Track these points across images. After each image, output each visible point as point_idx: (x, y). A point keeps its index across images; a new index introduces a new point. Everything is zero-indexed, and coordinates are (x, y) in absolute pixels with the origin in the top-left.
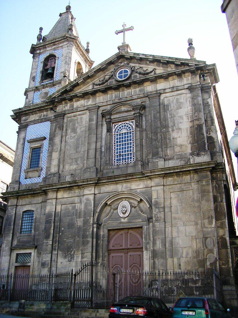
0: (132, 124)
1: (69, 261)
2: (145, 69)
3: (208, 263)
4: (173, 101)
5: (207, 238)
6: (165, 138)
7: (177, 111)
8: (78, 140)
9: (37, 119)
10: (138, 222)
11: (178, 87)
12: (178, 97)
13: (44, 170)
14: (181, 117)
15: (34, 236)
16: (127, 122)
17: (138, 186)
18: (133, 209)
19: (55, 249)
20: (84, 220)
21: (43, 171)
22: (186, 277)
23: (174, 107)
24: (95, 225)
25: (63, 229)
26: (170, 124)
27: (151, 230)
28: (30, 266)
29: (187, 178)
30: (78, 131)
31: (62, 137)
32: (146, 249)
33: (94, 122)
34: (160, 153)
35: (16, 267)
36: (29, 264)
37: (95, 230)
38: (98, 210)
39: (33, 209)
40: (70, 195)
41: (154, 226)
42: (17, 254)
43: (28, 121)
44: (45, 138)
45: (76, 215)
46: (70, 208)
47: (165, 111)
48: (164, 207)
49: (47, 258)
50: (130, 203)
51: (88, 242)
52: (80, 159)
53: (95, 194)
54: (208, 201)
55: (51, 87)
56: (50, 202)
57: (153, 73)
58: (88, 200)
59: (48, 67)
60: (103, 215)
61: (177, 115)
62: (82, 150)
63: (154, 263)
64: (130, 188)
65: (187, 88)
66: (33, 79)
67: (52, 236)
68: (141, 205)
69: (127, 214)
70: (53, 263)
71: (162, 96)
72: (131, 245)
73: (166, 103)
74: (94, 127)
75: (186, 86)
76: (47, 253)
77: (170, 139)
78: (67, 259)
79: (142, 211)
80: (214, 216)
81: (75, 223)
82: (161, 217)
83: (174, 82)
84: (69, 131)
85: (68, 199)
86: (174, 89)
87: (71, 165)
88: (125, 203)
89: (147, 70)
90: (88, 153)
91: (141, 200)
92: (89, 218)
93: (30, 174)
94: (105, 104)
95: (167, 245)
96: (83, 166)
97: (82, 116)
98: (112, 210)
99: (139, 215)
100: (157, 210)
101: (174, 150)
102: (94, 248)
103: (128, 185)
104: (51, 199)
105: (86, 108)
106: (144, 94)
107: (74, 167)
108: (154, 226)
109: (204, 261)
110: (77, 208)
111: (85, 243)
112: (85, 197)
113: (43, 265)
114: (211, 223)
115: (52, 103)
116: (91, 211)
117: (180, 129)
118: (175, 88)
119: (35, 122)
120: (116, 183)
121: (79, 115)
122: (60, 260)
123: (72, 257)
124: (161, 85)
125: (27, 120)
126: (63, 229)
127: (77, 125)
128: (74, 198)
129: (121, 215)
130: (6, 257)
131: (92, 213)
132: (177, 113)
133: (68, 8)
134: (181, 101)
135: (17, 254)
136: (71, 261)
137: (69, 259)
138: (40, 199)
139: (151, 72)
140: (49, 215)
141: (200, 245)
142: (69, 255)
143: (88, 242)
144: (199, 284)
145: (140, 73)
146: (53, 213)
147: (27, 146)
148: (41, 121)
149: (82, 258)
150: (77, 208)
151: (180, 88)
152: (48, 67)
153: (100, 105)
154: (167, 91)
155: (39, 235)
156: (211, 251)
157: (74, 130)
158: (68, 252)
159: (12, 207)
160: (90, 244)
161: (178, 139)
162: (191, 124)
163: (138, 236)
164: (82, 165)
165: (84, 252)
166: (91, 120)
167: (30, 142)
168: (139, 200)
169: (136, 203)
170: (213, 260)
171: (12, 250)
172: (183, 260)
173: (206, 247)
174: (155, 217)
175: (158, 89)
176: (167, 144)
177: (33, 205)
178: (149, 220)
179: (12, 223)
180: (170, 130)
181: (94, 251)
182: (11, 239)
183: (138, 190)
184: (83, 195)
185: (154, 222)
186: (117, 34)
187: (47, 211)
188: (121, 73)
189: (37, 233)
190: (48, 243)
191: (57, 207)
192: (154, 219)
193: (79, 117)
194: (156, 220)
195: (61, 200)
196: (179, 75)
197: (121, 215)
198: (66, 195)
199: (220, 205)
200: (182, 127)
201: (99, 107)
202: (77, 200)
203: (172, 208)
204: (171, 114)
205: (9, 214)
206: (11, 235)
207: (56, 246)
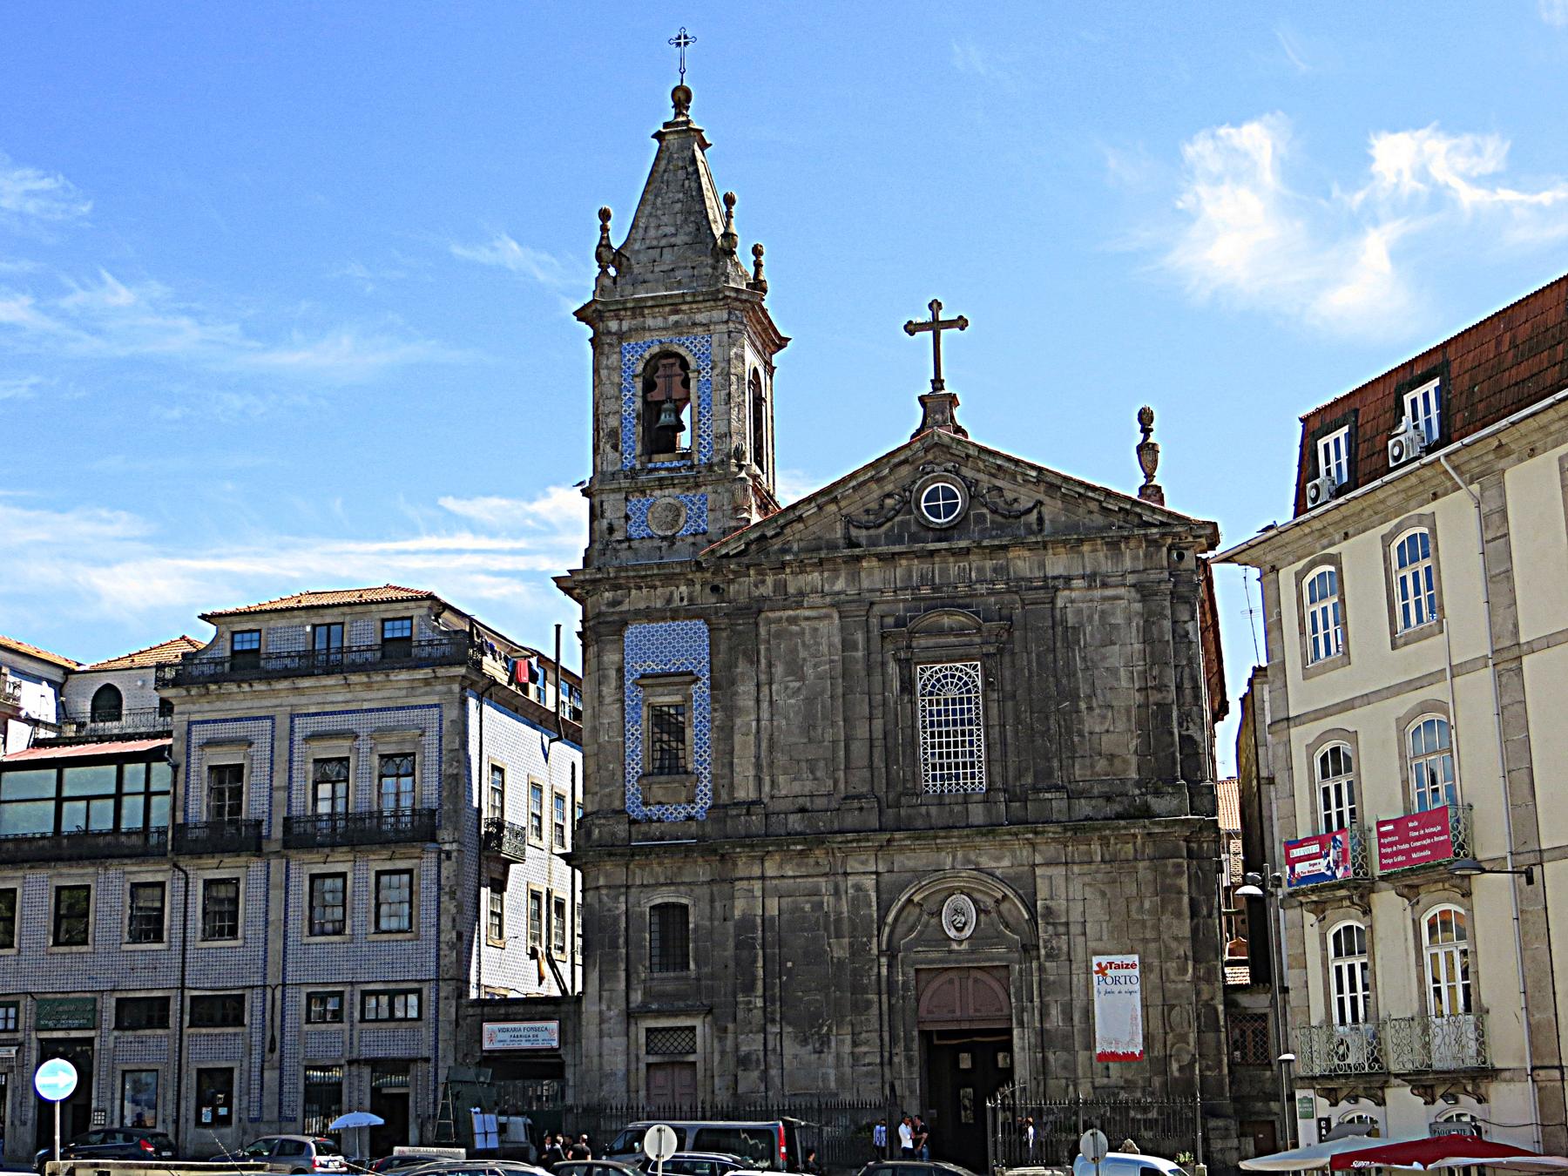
0: (973, 673)
2: (1009, 496)
3: (1175, 1066)
4: (1090, 618)
5: (1172, 1007)
6: (1069, 731)
7: (1103, 650)
8: (810, 701)
12: (1106, 606)
13: (705, 782)
14: (1113, 671)
15: (698, 979)
17: (1000, 859)
18: (982, 916)
19: (773, 1021)
20: (851, 945)
22: (1123, 1095)
23: (1092, 635)
24: (884, 960)
25: (789, 964)
27: (1035, 979)
28: (694, 1063)
30: (809, 671)
31: (758, 685)
32: (1021, 1024)
35: (649, 1066)
36: (691, 1058)
37: (884, 971)
38: (890, 919)
39: (684, 901)
40: (803, 871)
41: (1041, 969)
42: (648, 1030)
44: (691, 677)
45: (826, 929)
46: (808, 907)
47: (1069, 646)
48: (1067, 924)
49: (752, 1044)
50: (975, 902)
51: (869, 1004)
52: (822, 764)
53: (877, 873)
54: (1178, 914)
57: (1034, 515)
59: (656, 395)
60: (900, 930)
61: (1101, 665)
62: (828, 737)
63: (1044, 1059)
64: (977, 864)
65: (1134, 586)
66: (605, 438)
67: (760, 984)
68: (1005, 907)
69: (967, 932)
70: (772, 1058)
71: (1062, 598)
72: (976, 1010)
73: (1071, 620)
74: (860, 667)
75: (1131, 579)
78: (810, 1047)
79: (1007, 926)
80: (1190, 954)
82: (1059, 949)
83: (1095, 557)
84: (779, 670)
89: (1016, 500)
90: (847, 748)
91: (1005, 897)
93: (658, 792)
94: (889, 596)
95: (1076, 1018)
96: (836, 782)
97: (815, 624)
98: (925, 917)
99: (1000, 935)
100: (1050, 928)
101: (1092, 766)
102: (886, 1017)
108: (1041, 969)
109: (1166, 1059)
111: (861, 1007)
112: (851, 880)
113: (744, 1062)
115: (714, 566)
119: (649, 615)
122: (790, 1048)
123: (825, 1041)
124: (1057, 563)
125: (620, 603)
127: (803, 654)
129: (952, 933)
132: (1104, 658)
134: (1119, 619)
135: (648, 1030)
136: (821, 1052)
138: (701, 871)
139: (1030, 511)
140: (746, 924)
143: (869, 1004)
144: (1153, 1114)
146: (759, 921)
147: (633, 694)
149: (855, 1044)
152: (656, 395)
153: (876, 597)
154: (1076, 583)
155: (713, 976)
156: (1183, 1038)
157: (795, 669)
158: (812, 1030)
159: (613, 892)
160: (875, 1010)
162: (1138, 698)
163: (996, 986)
164: (830, 782)
165: (858, 1029)
166: (848, 645)
168: (999, 896)
169: (990, 903)
170: (1186, 1059)
171: (630, 1015)
173: (1172, 1030)
175: (1050, 574)
176: (1073, 749)
178: (1029, 949)
179: (621, 941)
180: (1083, 706)
181: (886, 1028)
182: (623, 985)
183: (998, 873)
184: (846, 874)
187: (737, 913)
188: (932, 496)
189: (706, 970)
190: (750, 1002)
191: (768, 901)
192: (1043, 952)
193: (804, 624)
197: (952, 933)
199: (1205, 924)
200: (1114, 703)
201: (872, 604)
203: (1088, 925)
204: (1084, 659)
206: (623, 975)
207: (773, 1012)
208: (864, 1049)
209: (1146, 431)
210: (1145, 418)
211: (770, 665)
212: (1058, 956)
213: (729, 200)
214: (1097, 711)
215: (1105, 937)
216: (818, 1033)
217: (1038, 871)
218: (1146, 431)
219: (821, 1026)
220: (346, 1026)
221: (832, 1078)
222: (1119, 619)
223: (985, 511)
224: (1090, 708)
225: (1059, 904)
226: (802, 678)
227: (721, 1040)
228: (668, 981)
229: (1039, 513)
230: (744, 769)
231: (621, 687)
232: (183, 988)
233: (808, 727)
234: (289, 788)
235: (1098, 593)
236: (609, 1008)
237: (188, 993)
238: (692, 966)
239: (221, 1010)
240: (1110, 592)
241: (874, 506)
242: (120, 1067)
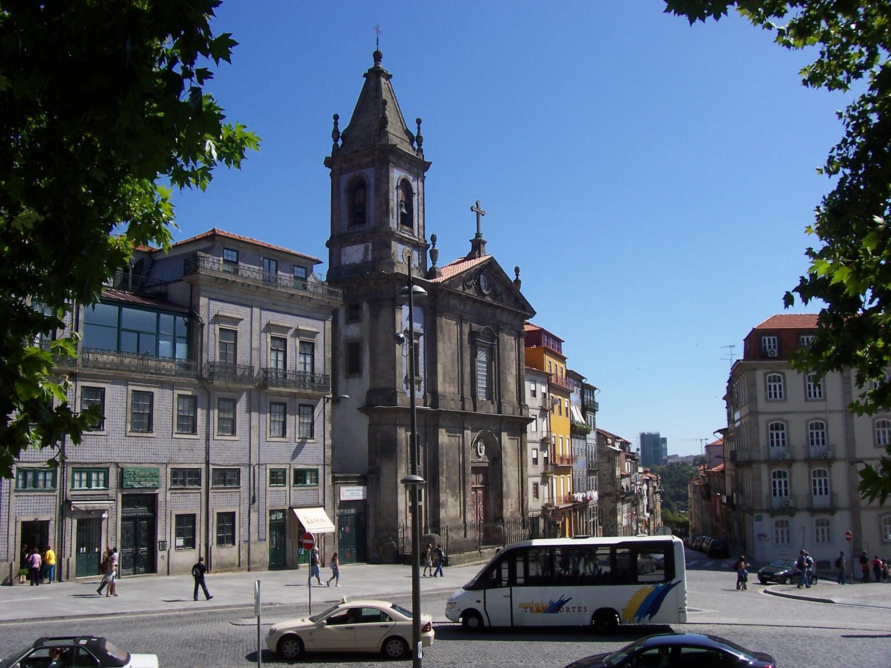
8: (453, 353)
75: (518, 329)
84: (446, 337)
133: (377, 56)
157: (450, 340)
209: (517, 275)
210: (517, 270)
213: (419, 121)
218: (517, 275)
220: (287, 488)
232: (207, 463)
233: (453, 365)
234: (260, 350)
237: (211, 467)
239: (227, 477)
242: (175, 512)
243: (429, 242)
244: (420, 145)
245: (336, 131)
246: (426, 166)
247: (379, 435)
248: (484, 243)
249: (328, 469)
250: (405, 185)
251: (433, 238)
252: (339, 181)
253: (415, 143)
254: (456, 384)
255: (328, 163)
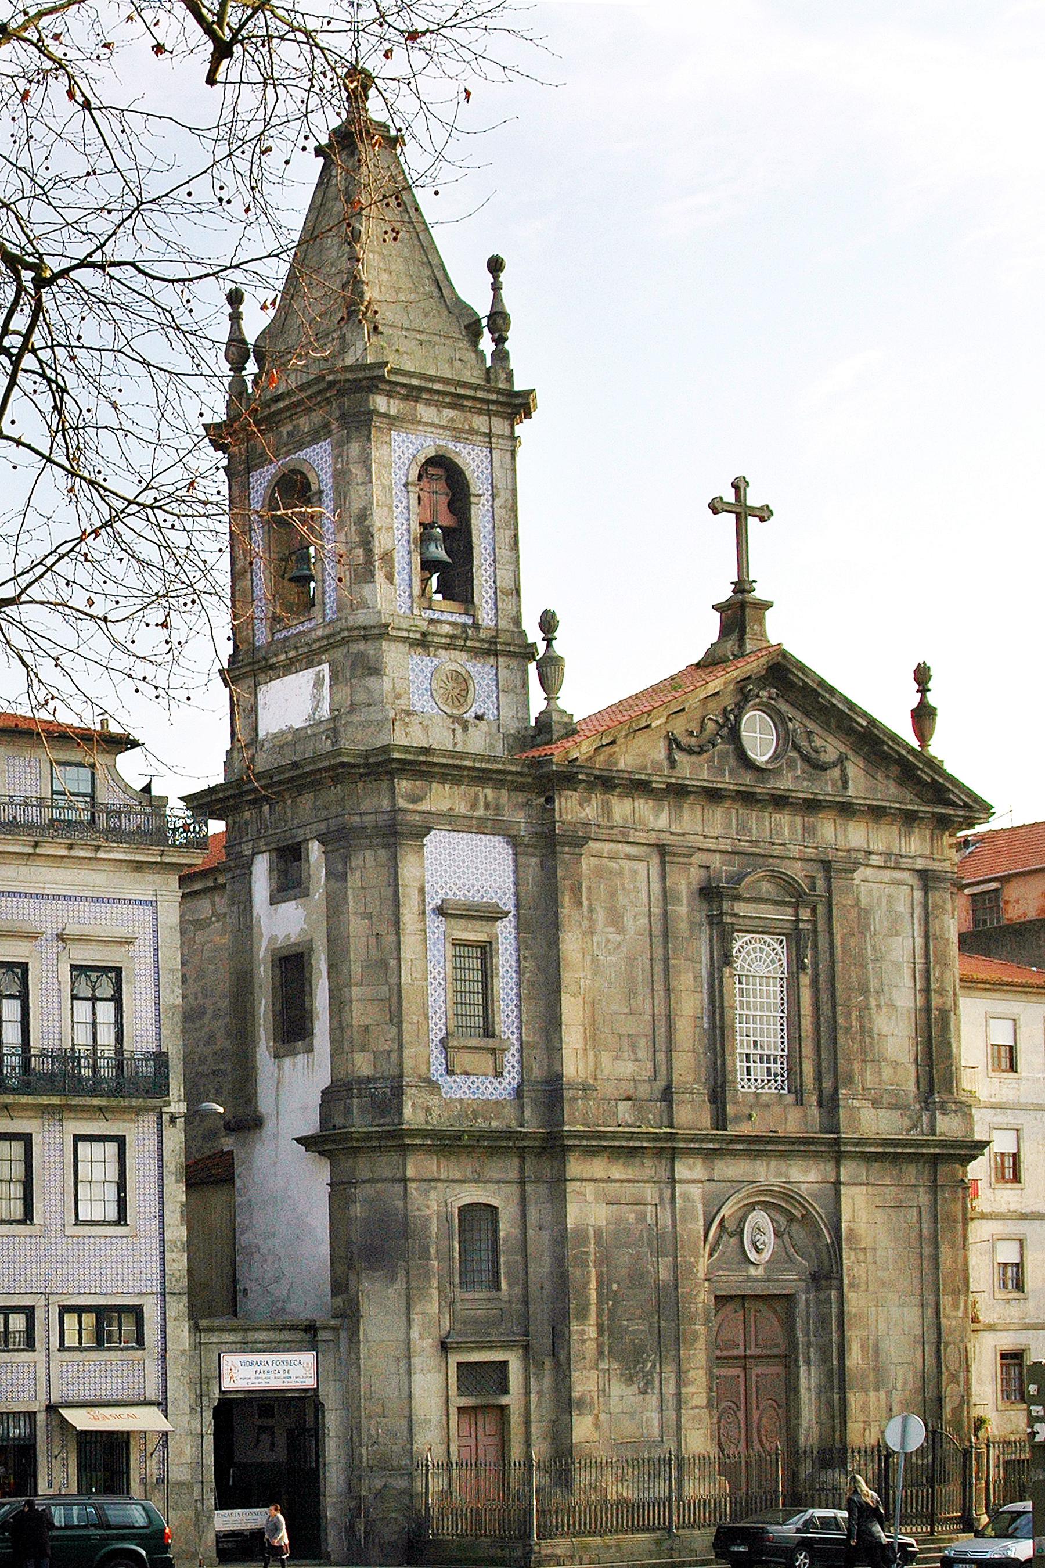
1: (641, 1393)
2: (818, 742)
5: (947, 1344)
8: (631, 960)
9: (462, 809)
10: (791, 1281)
11: (901, 856)
12: (892, 889)
13: (513, 1050)
14: (897, 966)
16: (766, 937)
17: (806, 1176)
21: (509, 1056)
23: (881, 922)
26: (873, 984)
29: (911, 1173)
33: (683, 910)
34: (857, 1078)
35: (459, 1408)
36: (504, 1400)
39: (493, 1202)
42: (459, 1364)
43: (423, 806)
44: (493, 915)
46: (632, 1217)
52: (642, 1041)
55: (476, 655)
56: (578, 1189)
57: (836, 773)
58: (687, 1198)
61: (888, 957)
63: (844, 1401)
67: (593, 1308)
69: (766, 1255)
74: (683, 926)
75: (920, 863)
76: (585, 1368)
77: (872, 1037)
81: (648, 1272)
84: (600, 916)
85: (625, 1184)
86: (893, 861)
87: (617, 1058)
88: (759, 1218)
92: (692, 1260)
94: (711, 844)
99: (791, 1260)
100: (853, 1253)
103: (783, 1166)
104: (582, 1180)
105: (652, 838)
106: (816, 848)
107: (627, 1068)
110: (649, 1222)
114: (956, 1306)
116: (699, 1237)
117: (893, 1006)
118: (893, 858)
120: (757, 1155)
121: (629, 857)
124: (857, 835)
126: (615, 1287)
127: (622, 899)
128: (642, 1184)
130: (429, 1376)
131: (702, 1243)
135: (459, 1364)
136: (645, 1393)
137: (642, 1384)
141: (930, 1360)
142: (641, 1374)
145: (806, 758)
147: (436, 926)
148: (481, 827)
150: (649, 1222)
151: (905, 863)
154: (875, 860)
157: (615, 919)
161: (890, 1039)
164: (650, 1065)
167: (440, 911)
171: (444, 1347)
172: (897, 1396)
174: (849, 1275)
177: (492, 1187)
185: (845, 1287)
186: (715, 511)
187: (570, 1222)
190: (582, 1332)
192: (846, 1281)
194: (851, 1285)
195: (604, 1185)
196: (909, 819)
197: (752, 1255)
198: (617, 1171)
200: (898, 1004)
202: (650, 1193)
203: (879, 1253)
204: (874, 947)
205: (417, 1213)
206: (435, 1292)
208: (691, 1389)
209: (923, 690)
210: (922, 676)
211: (591, 910)
212: (858, 1285)
214: (884, 1010)
215: (891, 1267)
216: (642, 1370)
217: (843, 1190)
218: (923, 690)
219: (644, 1362)
221: (656, 1423)
222: (902, 908)
223: (794, 754)
224: (878, 1006)
225: (862, 1228)
226: (621, 930)
227: (540, 1378)
228: (475, 1302)
229: (843, 770)
230: (572, 1037)
231: (424, 913)
235: (888, 875)
236: (421, 1338)
238: (504, 1285)
240: (898, 875)
241: (695, 728)
243: (534, 635)
244: (500, 340)
245: (236, 340)
246: (519, 406)
247: (357, 1210)
248: (766, 605)
249: (178, 1306)
250: (443, 472)
251: (548, 623)
252: (246, 487)
253: (487, 335)
254: (642, 1054)
255: (218, 435)
